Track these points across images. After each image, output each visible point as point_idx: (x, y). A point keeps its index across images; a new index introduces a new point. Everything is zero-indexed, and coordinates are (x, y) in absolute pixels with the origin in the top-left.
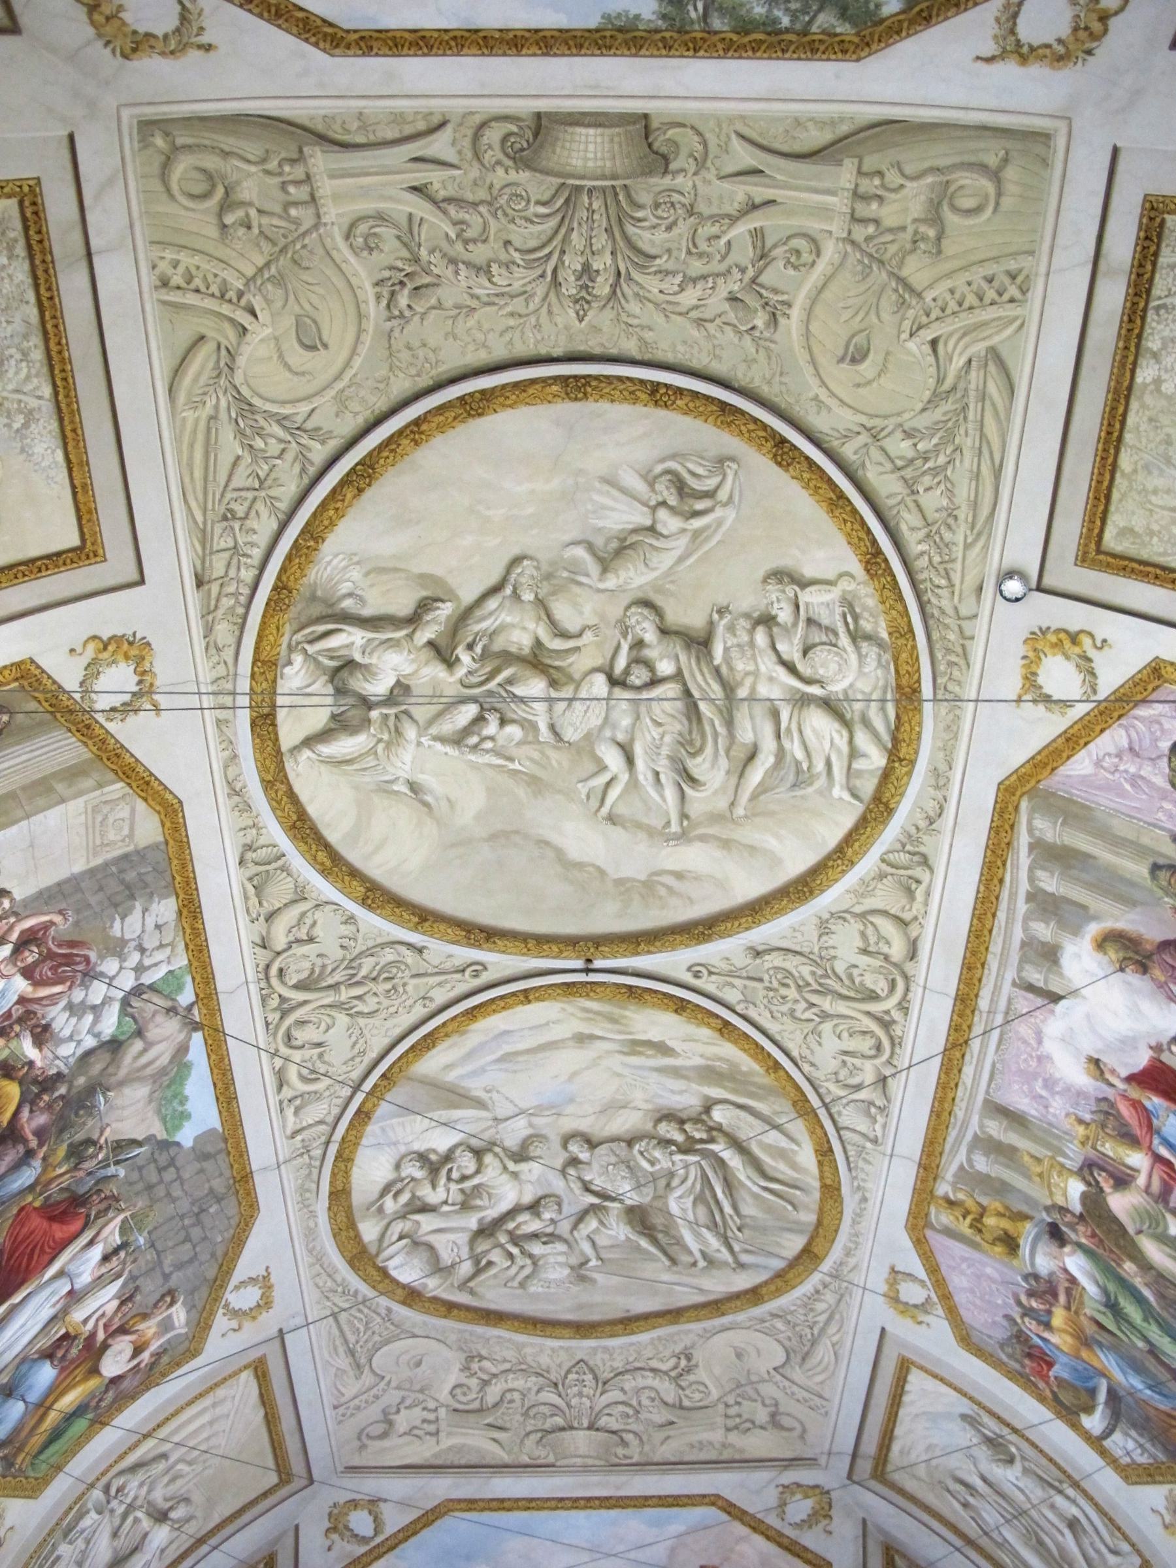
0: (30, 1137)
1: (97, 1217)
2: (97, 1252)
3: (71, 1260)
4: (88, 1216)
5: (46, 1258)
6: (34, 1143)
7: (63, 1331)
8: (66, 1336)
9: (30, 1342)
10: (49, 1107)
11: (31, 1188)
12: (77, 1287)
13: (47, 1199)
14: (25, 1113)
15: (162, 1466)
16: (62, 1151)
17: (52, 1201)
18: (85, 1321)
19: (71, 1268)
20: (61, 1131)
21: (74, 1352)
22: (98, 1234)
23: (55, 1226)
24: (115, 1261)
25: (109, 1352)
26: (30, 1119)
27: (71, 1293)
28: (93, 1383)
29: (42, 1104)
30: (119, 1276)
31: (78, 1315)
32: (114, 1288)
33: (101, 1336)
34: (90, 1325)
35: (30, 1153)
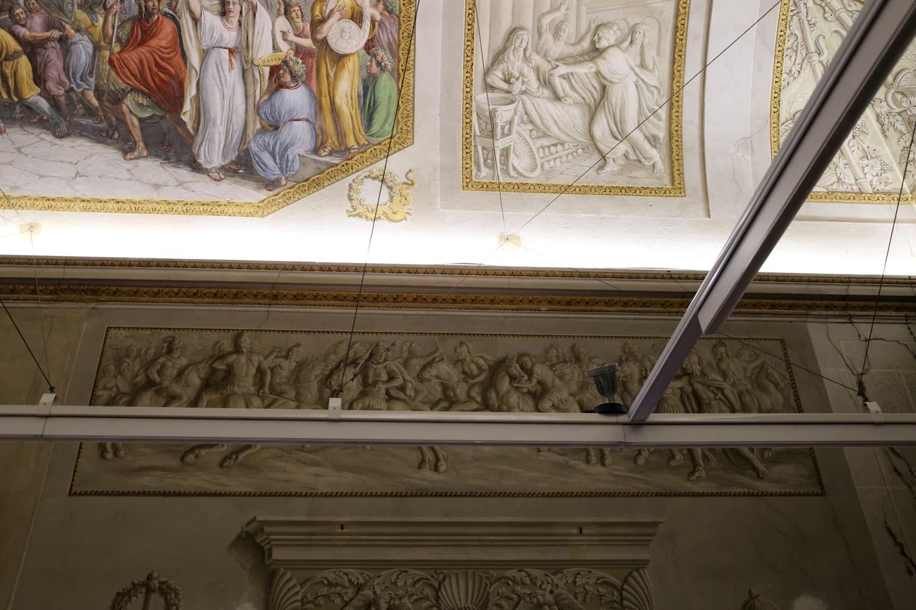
0: (48, 34)
1: (174, 10)
2: (211, 20)
3: (199, 40)
4: (165, 14)
5: (178, 59)
6: (56, 34)
7: (267, 71)
8: (274, 70)
9: (246, 97)
10: (29, 11)
11: (97, 48)
12: (231, 45)
13: (119, 40)
14: (22, 31)
15: (525, 38)
16: (82, 16)
17: (124, 38)
18: (275, 48)
19: (205, 44)
20: (61, 9)
21: (299, 67)
22: (191, 13)
23: (153, 43)
24: (235, 9)
25: (332, 42)
26: (30, 29)
27: (231, 51)
28: (351, 65)
29: (23, 16)
30: (254, 9)
31: (263, 53)
32: (263, 14)
33: (307, 42)
34: (284, 47)
35: (63, 41)
